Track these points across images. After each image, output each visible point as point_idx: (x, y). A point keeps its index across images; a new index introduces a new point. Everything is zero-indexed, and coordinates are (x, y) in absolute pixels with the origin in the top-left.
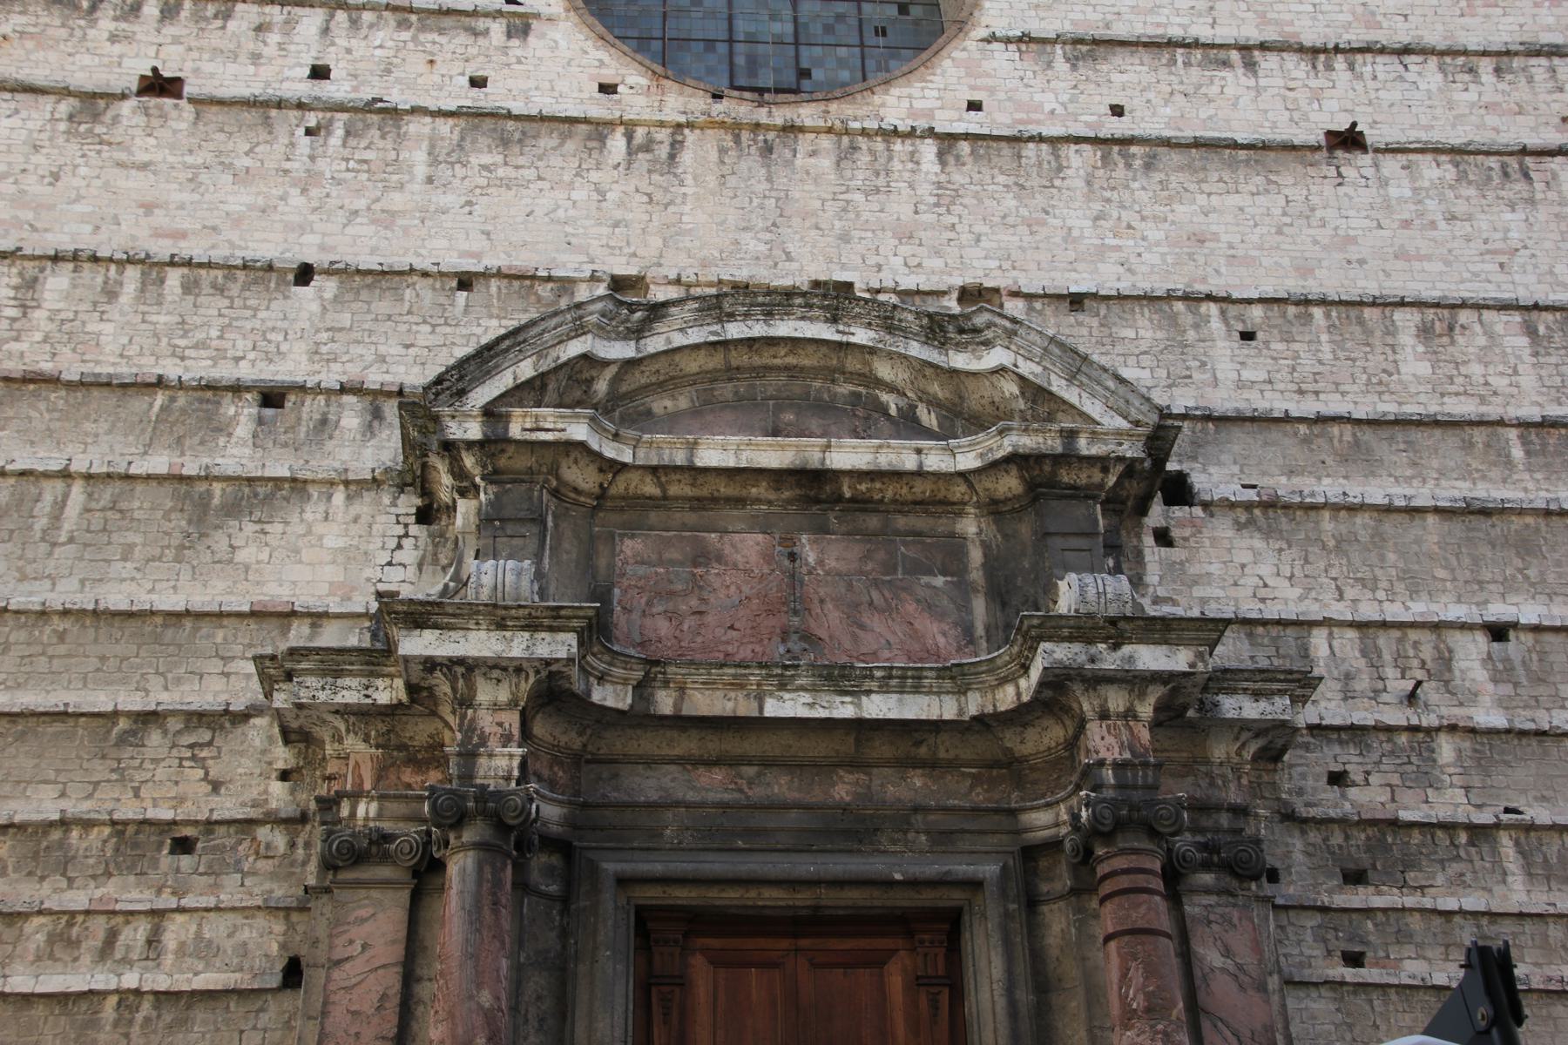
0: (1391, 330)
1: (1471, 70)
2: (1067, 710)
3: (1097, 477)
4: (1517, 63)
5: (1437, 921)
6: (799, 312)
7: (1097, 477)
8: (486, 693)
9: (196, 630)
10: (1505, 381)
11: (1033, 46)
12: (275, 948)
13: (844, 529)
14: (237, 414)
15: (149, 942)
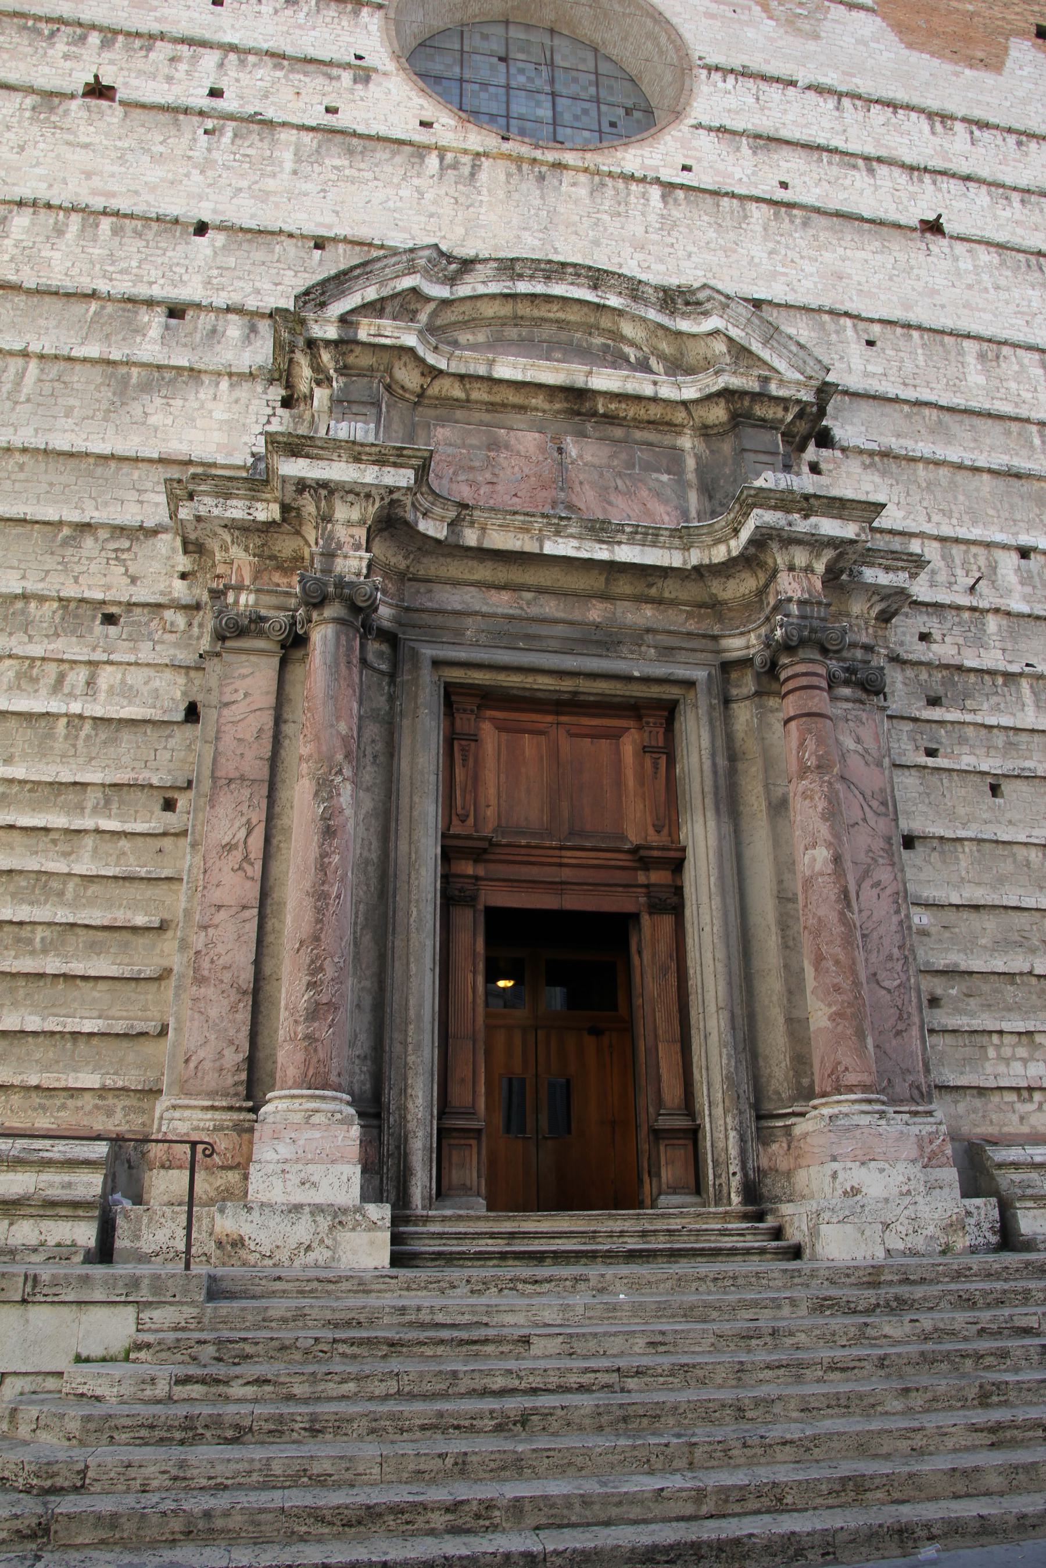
0: (961, 353)
1: (1007, 198)
2: (762, 565)
3: (780, 414)
4: (1034, 198)
5: (984, 732)
6: (570, 279)
7: (780, 414)
8: (342, 512)
9: (119, 469)
10: (1030, 395)
11: (727, 136)
12: (178, 695)
13: (597, 435)
14: (150, 321)
15: (88, 684)
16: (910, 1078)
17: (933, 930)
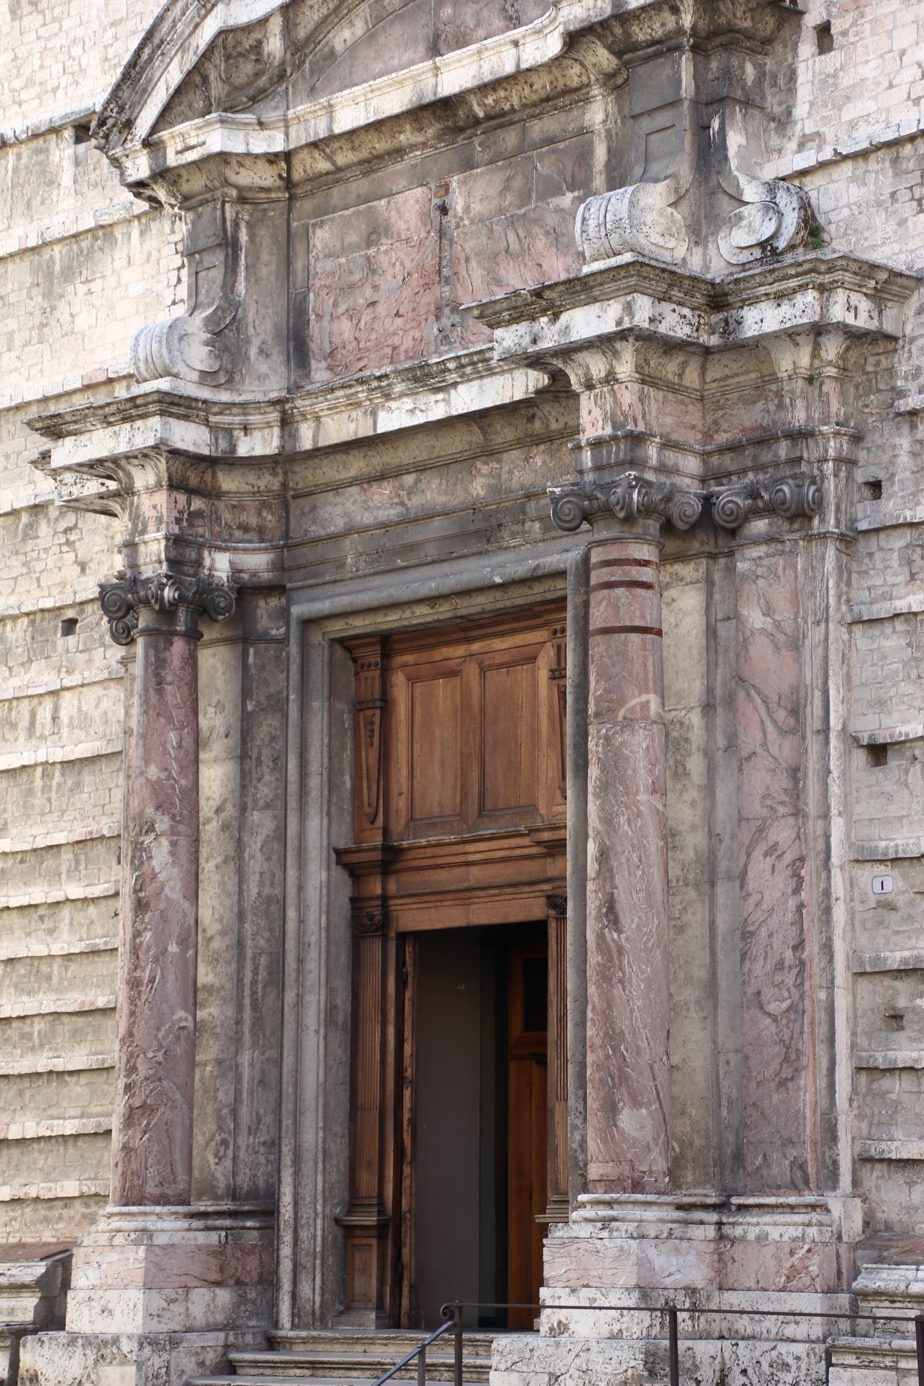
3: (671, 22)
7: (671, 22)
16: (792, 1152)
17: (901, 901)
